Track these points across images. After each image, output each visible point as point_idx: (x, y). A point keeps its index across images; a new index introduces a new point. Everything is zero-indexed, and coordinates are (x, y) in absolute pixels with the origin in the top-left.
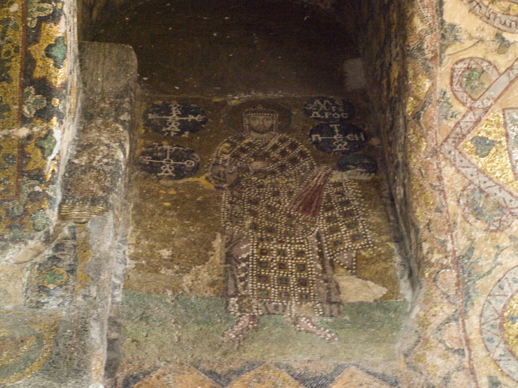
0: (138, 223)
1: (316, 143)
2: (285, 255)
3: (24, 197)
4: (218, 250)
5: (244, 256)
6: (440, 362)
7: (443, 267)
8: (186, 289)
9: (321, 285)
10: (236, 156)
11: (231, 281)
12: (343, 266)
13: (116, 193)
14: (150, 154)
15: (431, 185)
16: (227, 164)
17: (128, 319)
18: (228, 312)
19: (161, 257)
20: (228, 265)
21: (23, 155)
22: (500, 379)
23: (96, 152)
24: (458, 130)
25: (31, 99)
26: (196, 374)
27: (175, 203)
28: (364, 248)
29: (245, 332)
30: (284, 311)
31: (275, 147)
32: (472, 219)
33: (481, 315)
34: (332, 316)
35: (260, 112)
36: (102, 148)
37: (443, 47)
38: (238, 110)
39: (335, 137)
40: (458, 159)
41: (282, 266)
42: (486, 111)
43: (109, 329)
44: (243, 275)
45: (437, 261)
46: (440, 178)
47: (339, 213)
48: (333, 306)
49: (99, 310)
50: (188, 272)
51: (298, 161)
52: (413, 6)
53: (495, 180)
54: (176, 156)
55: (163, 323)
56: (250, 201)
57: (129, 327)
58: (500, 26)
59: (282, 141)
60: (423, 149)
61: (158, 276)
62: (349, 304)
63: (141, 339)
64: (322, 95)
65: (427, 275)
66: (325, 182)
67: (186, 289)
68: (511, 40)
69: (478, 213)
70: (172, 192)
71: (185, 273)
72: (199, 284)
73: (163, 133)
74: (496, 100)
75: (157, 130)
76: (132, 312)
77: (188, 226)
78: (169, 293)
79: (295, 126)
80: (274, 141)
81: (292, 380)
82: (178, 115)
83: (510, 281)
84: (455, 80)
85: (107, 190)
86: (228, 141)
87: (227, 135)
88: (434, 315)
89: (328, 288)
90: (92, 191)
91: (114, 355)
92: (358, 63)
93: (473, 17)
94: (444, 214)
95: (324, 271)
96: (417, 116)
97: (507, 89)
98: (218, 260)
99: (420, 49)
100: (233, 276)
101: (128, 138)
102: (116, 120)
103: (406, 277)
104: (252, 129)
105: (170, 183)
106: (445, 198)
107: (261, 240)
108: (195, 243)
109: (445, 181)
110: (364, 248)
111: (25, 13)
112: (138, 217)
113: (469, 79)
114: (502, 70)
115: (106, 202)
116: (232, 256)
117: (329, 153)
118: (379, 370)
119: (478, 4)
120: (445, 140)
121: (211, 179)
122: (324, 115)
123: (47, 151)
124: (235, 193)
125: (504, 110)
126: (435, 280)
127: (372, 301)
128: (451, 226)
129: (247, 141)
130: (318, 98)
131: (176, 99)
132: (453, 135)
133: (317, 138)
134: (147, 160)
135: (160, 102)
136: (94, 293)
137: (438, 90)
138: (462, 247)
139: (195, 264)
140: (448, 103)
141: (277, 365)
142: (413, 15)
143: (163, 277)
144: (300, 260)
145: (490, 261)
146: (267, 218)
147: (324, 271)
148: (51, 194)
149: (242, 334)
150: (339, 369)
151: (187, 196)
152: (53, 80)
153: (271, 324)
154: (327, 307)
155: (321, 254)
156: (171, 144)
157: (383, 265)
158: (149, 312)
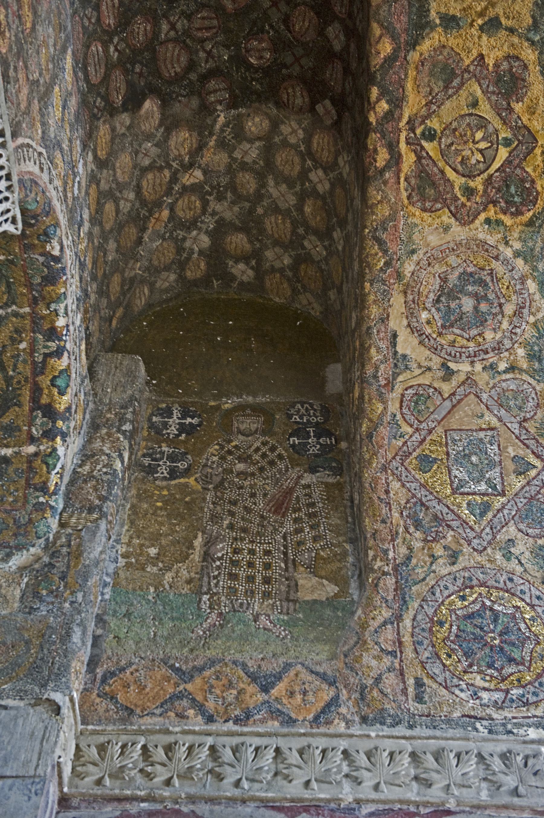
0: (132, 522)
1: (293, 446)
2: (254, 555)
3: (29, 507)
4: (198, 549)
5: (220, 555)
6: (374, 663)
7: (385, 574)
8: (167, 586)
9: (282, 582)
10: (223, 458)
11: (206, 579)
12: (303, 565)
13: (110, 501)
14: (150, 455)
15: (379, 498)
16: (215, 466)
17: (113, 616)
18: (199, 609)
19: (148, 555)
20: (205, 563)
21: (31, 468)
22: (425, 680)
23: (97, 462)
24: (405, 448)
25: (38, 421)
26: (164, 670)
27: (166, 503)
28: (323, 548)
29: (212, 629)
30: (247, 608)
31: (257, 450)
32: (412, 529)
33: (414, 620)
34: (288, 614)
35: (249, 415)
36: (103, 458)
37: (395, 375)
38: (229, 413)
39: (310, 441)
40: (404, 475)
41: (251, 565)
42: (430, 432)
43: (96, 625)
44: (216, 573)
45: (380, 568)
46: (387, 492)
47: (305, 514)
48: (291, 604)
49: (83, 615)
50: (170, 569)
51: (276, 463)
52: (370, 338)
53: (435, 494)
54: (172, 458)
55: (143, 618)
56: (230, 502)
57: (113, 623)
58: (446, 356)
59: (264, 444)
60: (374, 465)
61: (144, 574)
62: (304, 601)
63: (122, 636)
64: (304, 399)
65: (370, 580)
66: (296, 484)
67: (167, 586)
68: (455, 369)
69: (418, 525)
70: (165, 492)
71: (167, 570)
72: (178, 581)
73: (164, 435)
74: (439, 423)
75: (159, 432)
76: (118, 609)
77: (175, 525)
78: (152, 590)
79: (277, 430)
80: (257, 444)
81: (245, 678)
82: (178, 418)
83: (442, 588)
84: (404, 404)
85: (104, 499)
86: (218, 444)
87: (217, 438)
88: (373, 619)
89: (289, 586)
90: (90, 500)
91: (97, 651)
92: (339, 367)
93: (423, 348)
94: (388, 525)
95: (286, 570)
96: (370, 436)
97: (449, 412)
98: (197, 559)
99: (375, 377)
100: (208, 574)
101: (127, 448)
102: (119, 431)
103: (356, 578)
104: (240, 432)
105: (164, 483)
106: (390, 510)
107: (235, 539)
108: (179, 542)
109: (391, 495)
110: (323, 548)
111: (32, 349)
112: (133, 517)
113: (416, 403)
114: (446, 395)
115: (101, 510)
116: (208, 555)
117: (303, 456)
118: (320, 669)
119: (427, 337)
120: (394, 458)
121: (199, 480)
122: (303, 419)
123: (51, 467)
124: (219, 494)
125: (446, 431)
126: (376, 585)
127: (324, 599)
128: (394, 536)
129: (234, 444)
130: (298, 402)
131: (178, 403)
132: (401, 453)
133: (294, 441)
134: (147, 461)
135: (164, 405)
136: (80, 599)
137: (389, 413)
138: (401, 556)
139: (177, 562)
140: (398, 425)
141: (235, 663)
142: (370, 346)
143: (148, 575)
144: (267, 559)
145: (425, 569)
146: (243, 519)
147: (286, 570)
148: (53, 504)
149: (209, 631)
150: (287, 666)
151: (177, 496)
152: (57, 406)
153: (234, 621)
154: (285, 604)
155: (285, 554)
156: (169, 446)
157: (338, 565)
158: (132, 609)
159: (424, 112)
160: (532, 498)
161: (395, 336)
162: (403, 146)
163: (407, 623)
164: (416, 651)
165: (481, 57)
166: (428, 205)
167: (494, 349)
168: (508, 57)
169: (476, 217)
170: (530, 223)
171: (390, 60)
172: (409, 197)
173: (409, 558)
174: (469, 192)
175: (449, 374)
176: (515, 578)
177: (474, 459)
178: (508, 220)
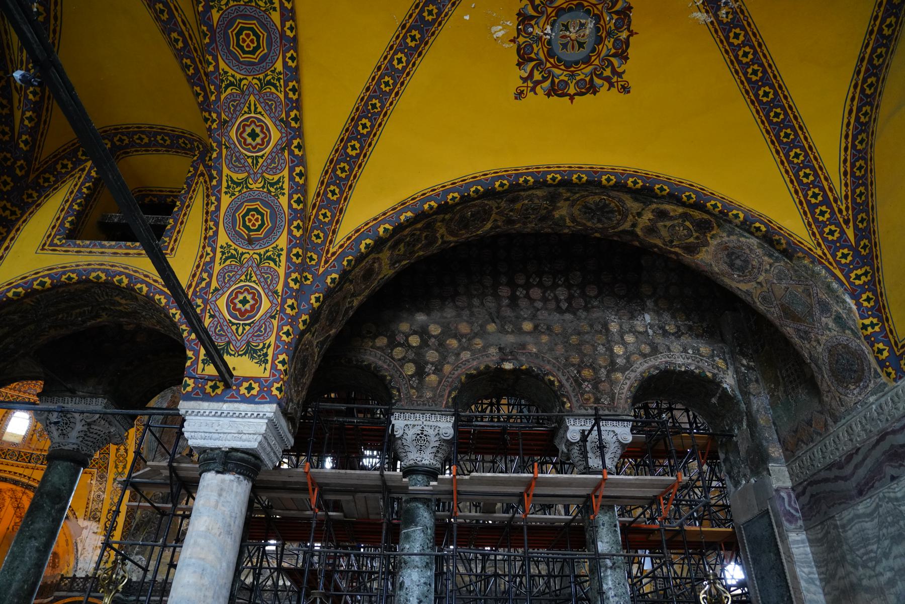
162: (672, 250)
163: (826, 376)
165: (649, 220)
168: (652, 212)
171: (640, 243)
174: (697, 238)
178: (714, 232)
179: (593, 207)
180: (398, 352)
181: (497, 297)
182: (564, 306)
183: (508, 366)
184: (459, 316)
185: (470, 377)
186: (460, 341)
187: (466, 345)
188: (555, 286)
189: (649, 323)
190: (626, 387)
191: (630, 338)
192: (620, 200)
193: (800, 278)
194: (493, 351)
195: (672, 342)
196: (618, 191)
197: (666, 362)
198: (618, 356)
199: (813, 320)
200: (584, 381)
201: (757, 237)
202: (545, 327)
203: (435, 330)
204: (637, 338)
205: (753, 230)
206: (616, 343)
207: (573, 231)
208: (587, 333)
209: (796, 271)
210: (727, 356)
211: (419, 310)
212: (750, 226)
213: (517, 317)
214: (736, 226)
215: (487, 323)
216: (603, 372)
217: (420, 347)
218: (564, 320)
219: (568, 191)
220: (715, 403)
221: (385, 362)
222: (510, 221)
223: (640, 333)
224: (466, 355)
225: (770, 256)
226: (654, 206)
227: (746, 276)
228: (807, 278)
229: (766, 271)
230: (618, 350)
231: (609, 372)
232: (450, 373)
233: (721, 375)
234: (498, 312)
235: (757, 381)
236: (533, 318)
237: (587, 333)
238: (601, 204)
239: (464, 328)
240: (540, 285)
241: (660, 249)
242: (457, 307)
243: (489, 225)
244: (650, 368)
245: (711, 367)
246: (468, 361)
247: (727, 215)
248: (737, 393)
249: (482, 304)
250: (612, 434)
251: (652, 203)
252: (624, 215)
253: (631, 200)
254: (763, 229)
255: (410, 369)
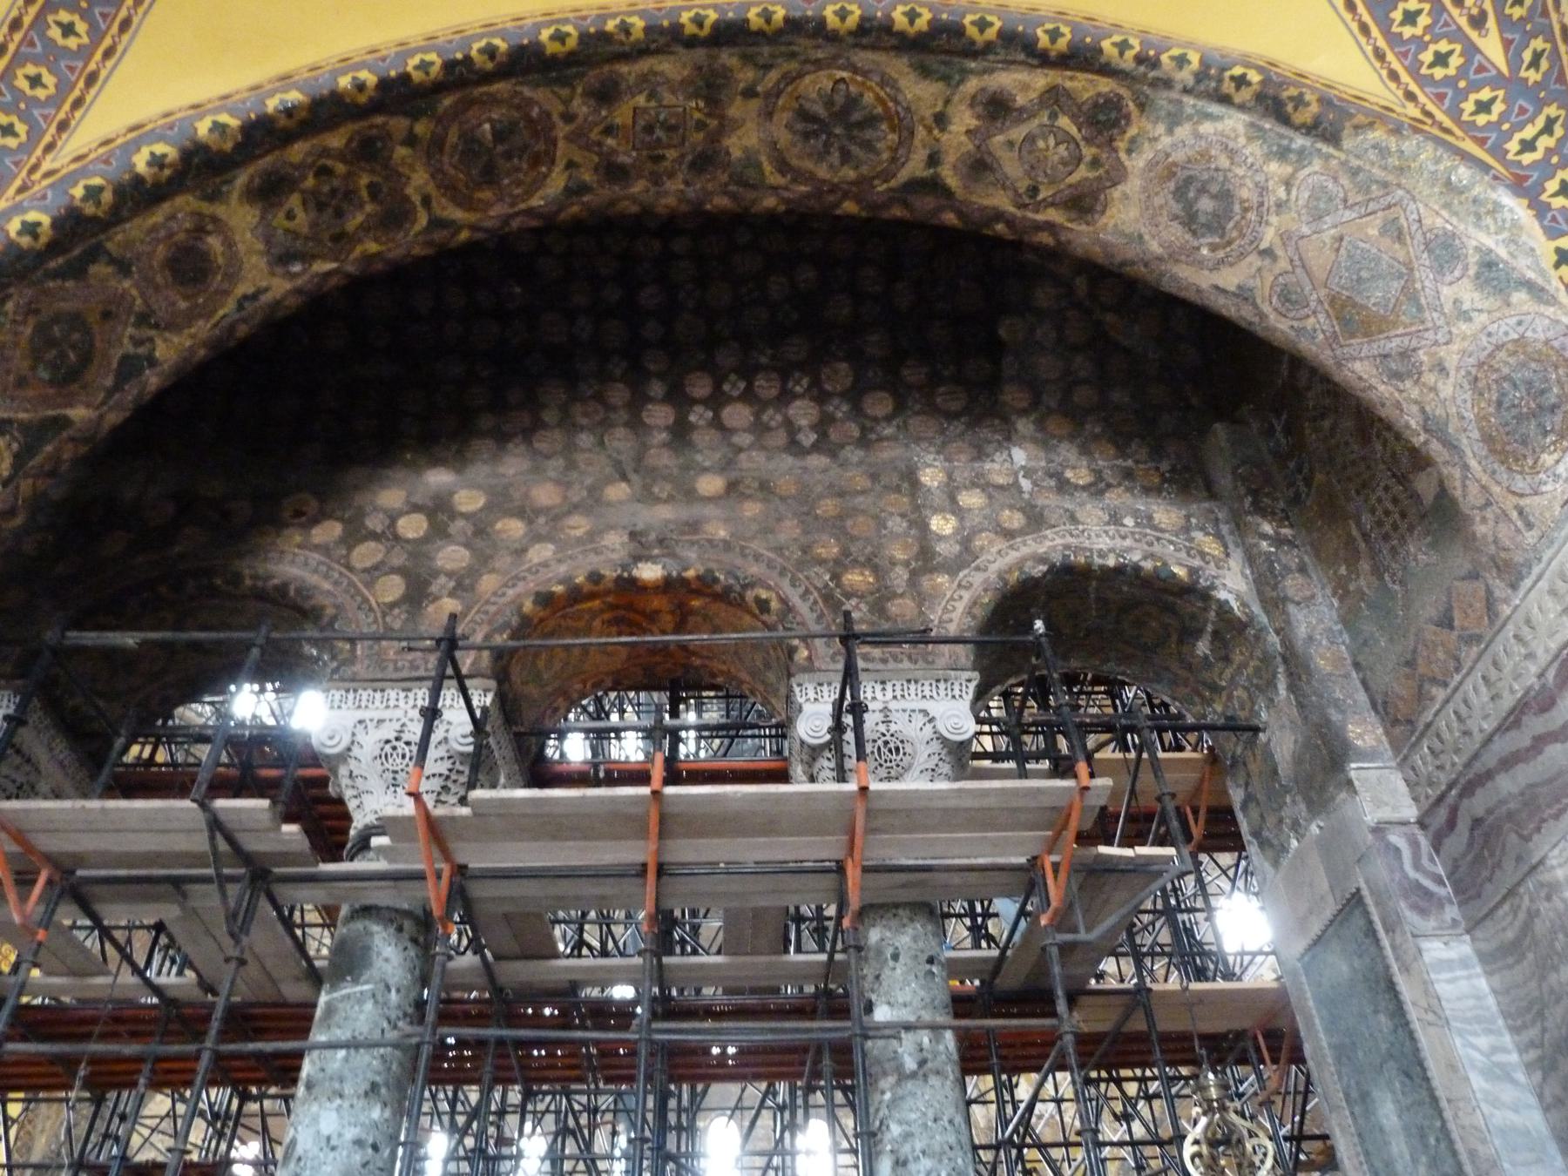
46: (1360, 378)
159: (1010, 193)
160: (1427, 245)
161: (1217, 287)
162: (1040, 217)
163: (1473, 463)
164: (1498, 483)
165: (968, 132)
166: (1099, 208)
167: (1261, 195)
168: (972, 106)
169: (1122, 164)
170: (1142, 107)
171: (960, 214)
172: (1088, 224)
173: (1423, 410)
174: (1095, 163)
175: (1268, 253)
176: (1490, 329)
177: (1364, 274)
178: (1132, 131)
179: (819, 110)
180: (366, 554)
181: (636, 424)
182: (808, 438)
183: (649, 572)
184: (537, 470)
185: (545, 600)
186: (530, 522)
187: (544, 531)
188: (785, 397)
189: (1023, 467)
190: (960, 607)
191: (971, 499)
192: (885, 81)
193: (1368, 191)
194: (616, 542)
195: (1082, 505)
196: (874, 48)
197: (1067, 547)
198: (941, 538)
199: (1420, 309)
200: (849, 596)
201: (1242, 107)
202: (756, 485)
203: (469, 501)
204: (990, 497)
205: (1228, 87)
206: (936, 510)
207: (787, 201)
208: (863, 492)
209: (1355, 172)
210: (1225, 529)
211: (436, 462)
212: (1220, 81)
213: (686, 468)
214: (1186, 91)
215: (609, 481)
216: (900, 576)
217: (425, 540)
218: (805, 469)
219: (747, 59)
220: (1206, 657)
221: (326, 577)
222: (614, 172)
223: (1001, 488)
224: (542, 552)
225: (1283, 154)
226: (972, 85)
227: (1229, 243)
228: (1385, 185)
229: (1280, 206)
230: (942, 524)
231: (914, 574)
232: (495, 594)
233: (1211, 570)
234: (639, 459)
235: (1302, 569)
236: (726, 466)
237: (863, 492)
238: (839, 99)
239: (545, 495)
240: (748, 396)
241: (1010, 222)
242: (536, 453)
243: (557, 182)
244: (1024, 560)
245: (1183, 555)
246: (545, 565)
247: (1155, 64)
248: (1256, 609)
249: (601, 443)
250: (919, 720)
251: (965, 73)
252: (903, 126)
253: (912, 76)
254: (1254, 77)
255: (392, 588)
